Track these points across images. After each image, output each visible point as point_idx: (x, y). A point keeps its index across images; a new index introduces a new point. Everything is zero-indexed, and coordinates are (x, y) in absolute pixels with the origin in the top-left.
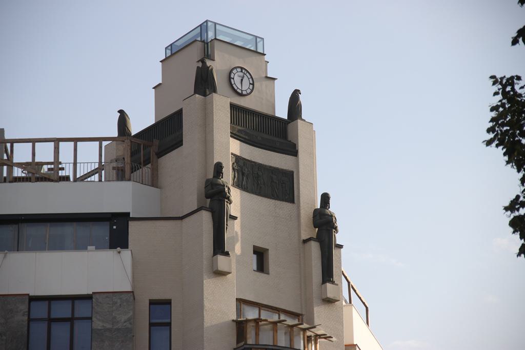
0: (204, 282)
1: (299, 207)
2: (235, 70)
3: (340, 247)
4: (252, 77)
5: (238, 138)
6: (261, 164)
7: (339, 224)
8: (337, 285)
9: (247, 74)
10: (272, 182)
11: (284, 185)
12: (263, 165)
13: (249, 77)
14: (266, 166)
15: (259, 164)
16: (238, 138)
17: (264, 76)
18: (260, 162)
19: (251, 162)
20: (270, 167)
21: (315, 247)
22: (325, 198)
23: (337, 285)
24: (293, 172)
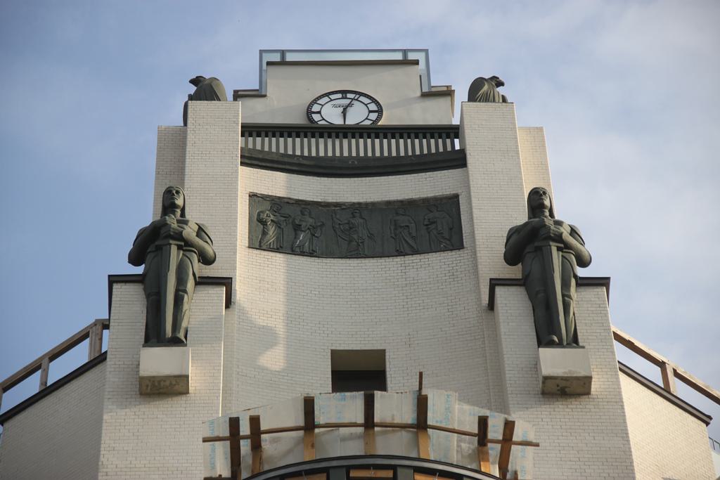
0: (105, 417)
1: (475, 253)
2: (351, 121)
3: (603, 282)
4: (374, 101)
5: (276, 166)
6: (359, 204)
7: (590, 247)
8: (583, 347)
9: (362, 99)
10: (395, 229)
11: (433, 226)
12: (367, 204)
13: (366, 101)
14: (373, 204)
15: (354, 204)
16: (276, 166)
17: (419, 94)
18: (356, 201)
19: (327, 205)
20: (389, 203)
21: (513, 304)
22: (537, 201)
23: (583, 347)
24: (456, 196)
